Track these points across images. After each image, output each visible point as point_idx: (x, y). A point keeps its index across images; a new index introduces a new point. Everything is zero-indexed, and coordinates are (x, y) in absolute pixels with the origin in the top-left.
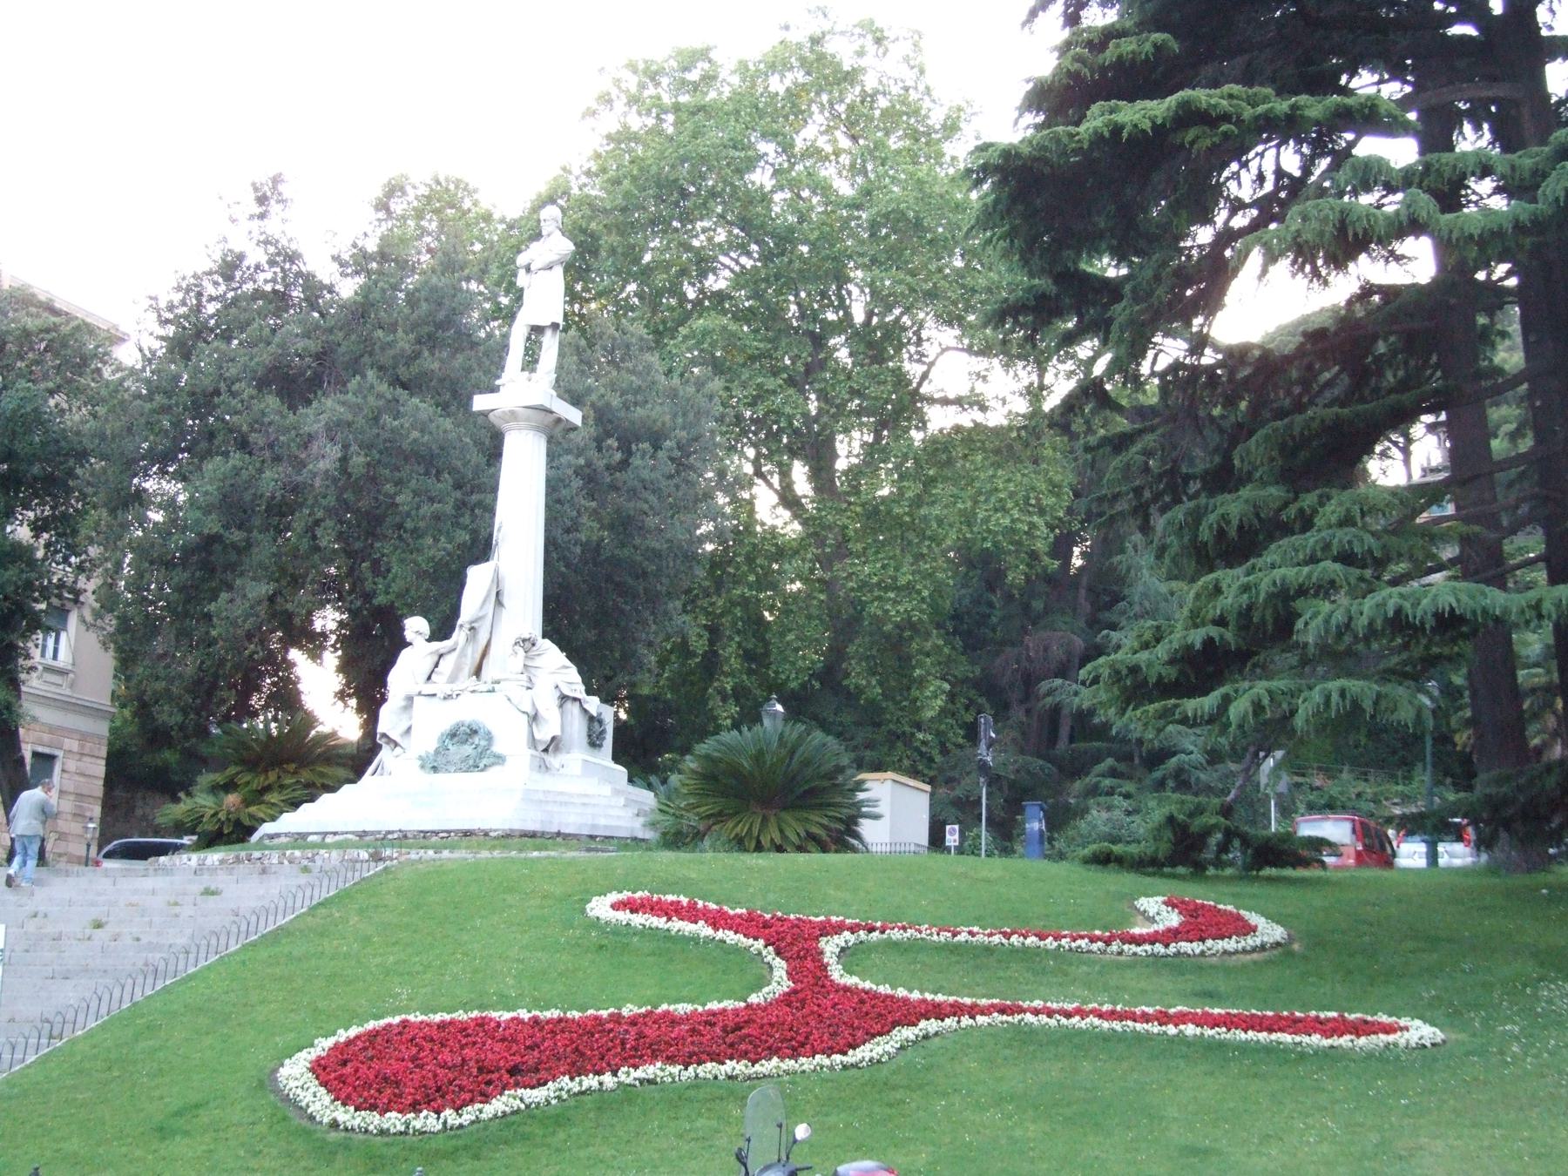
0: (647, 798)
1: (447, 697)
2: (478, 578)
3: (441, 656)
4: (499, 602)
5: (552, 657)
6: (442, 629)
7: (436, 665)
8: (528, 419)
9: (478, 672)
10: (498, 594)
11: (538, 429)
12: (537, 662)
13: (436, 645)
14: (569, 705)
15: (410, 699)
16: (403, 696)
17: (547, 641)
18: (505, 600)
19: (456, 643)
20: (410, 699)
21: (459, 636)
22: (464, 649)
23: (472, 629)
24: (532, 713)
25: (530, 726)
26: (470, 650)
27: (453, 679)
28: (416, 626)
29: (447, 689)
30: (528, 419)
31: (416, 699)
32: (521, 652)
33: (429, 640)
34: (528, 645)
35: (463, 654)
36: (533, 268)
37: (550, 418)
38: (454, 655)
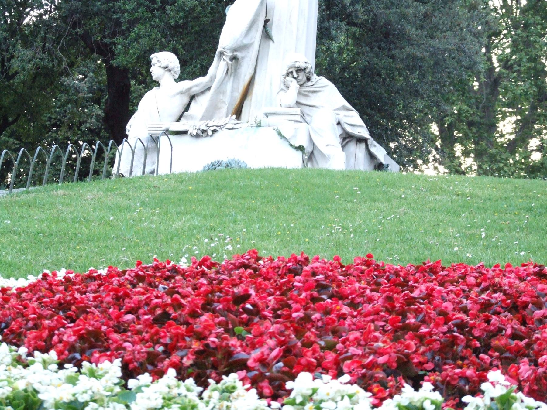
0: (307, 403)
1: (202, 134)
3: (192, 98)
4: (267, 35)
5: (329, 97)
7: (187, 109)
9: (238, 112)
10: (266, 21)
12: (312, 100)
13: (186, 84)
15: (155, 140)
17: (323, 81)
18: (274, 33)
21: (218, 68)
22: (222, 83)
23: (234, 58)
24: (309, 149)
26: (229, 86)
27: (209, 114)
31: (164, 140)
32: (294, 85)
34: (302, 77)
35: (220, 90)
38: (208, 95)
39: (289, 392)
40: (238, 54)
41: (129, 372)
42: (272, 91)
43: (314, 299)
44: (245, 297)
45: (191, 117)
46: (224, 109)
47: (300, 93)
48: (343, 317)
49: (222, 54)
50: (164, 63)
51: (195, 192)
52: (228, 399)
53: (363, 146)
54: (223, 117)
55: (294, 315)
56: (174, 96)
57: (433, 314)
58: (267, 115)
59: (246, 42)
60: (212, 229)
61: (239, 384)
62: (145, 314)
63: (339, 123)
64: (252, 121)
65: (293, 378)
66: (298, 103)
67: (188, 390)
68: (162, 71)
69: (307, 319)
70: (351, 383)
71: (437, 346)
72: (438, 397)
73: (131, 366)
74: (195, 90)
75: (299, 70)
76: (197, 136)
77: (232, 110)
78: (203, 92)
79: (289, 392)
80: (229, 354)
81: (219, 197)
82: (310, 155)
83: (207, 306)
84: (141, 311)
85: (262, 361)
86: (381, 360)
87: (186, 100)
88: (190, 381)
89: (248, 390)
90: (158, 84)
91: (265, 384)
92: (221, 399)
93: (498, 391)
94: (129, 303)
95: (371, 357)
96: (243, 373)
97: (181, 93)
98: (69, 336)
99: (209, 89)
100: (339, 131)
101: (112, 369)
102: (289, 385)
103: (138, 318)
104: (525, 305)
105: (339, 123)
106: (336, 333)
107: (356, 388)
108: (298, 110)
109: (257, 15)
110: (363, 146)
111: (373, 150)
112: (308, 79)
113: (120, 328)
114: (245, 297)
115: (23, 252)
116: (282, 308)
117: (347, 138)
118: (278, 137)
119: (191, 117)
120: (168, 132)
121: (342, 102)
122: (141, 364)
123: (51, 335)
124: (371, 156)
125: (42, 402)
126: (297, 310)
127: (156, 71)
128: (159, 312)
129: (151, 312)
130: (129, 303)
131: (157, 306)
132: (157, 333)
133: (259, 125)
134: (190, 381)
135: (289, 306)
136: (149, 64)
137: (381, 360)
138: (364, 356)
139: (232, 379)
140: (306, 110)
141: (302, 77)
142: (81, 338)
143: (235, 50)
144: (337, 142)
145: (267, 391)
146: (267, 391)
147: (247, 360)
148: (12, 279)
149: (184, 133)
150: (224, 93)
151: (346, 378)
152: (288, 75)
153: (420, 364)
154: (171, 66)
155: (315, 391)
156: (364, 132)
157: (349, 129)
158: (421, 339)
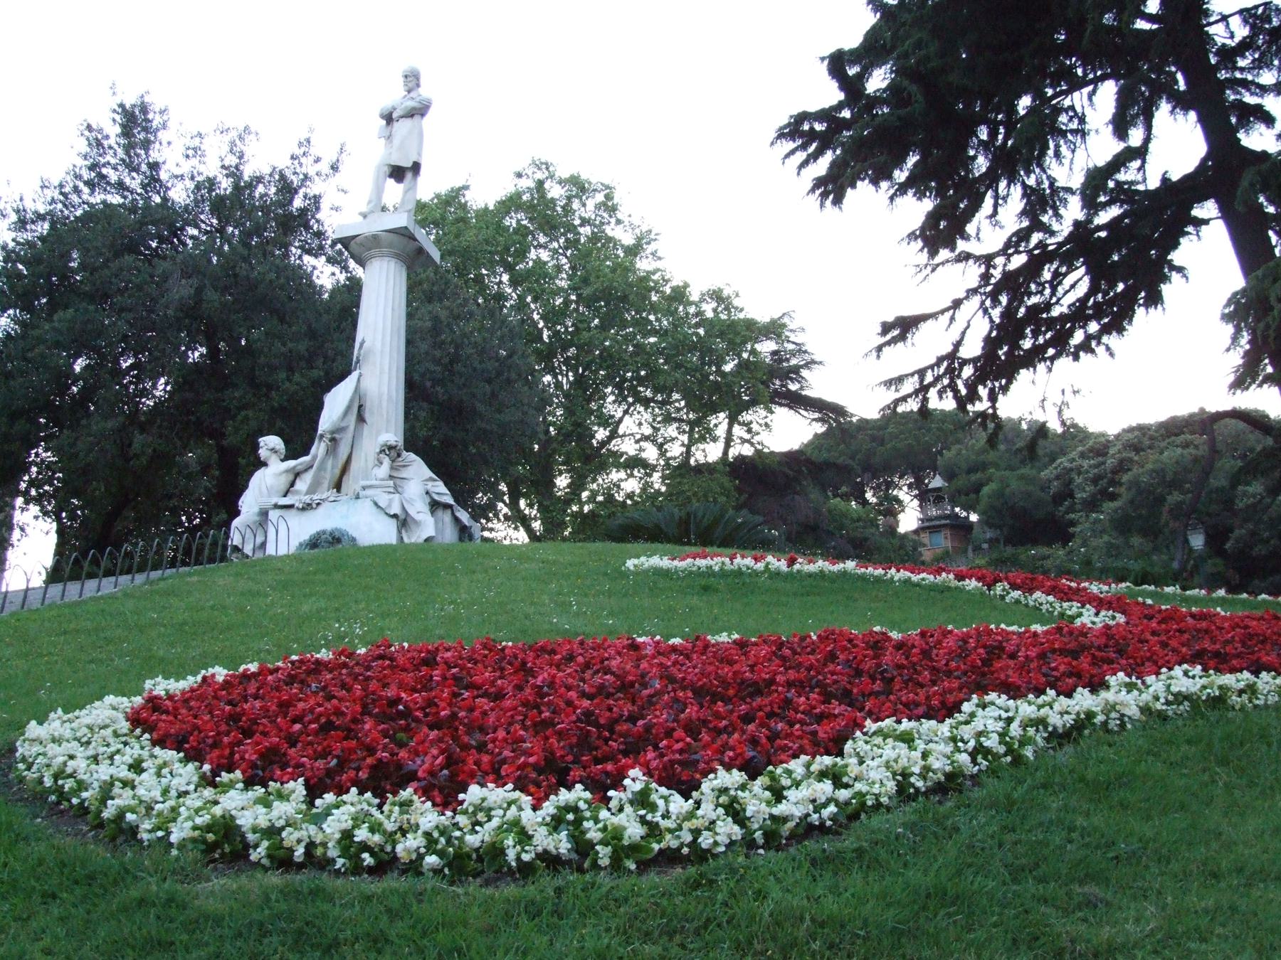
1: (307, 507)
2: (336, 402)
3: (297, 475)
4: (361, 419)
6: (297, 446)
7: (292, 485)
8: (390, 246)
9: (338, 486)
10: (360, 406)
11: (397, 256)
13: (292, 463)
14: (440, 513)
15: (264, 514)
16: (256, 510)
17: (412, 456)
18: (367, 416)
19: (315, 458)
20: (264, 514)
21: (319, 449)
22: (323, 462)
23: (333, 440)
24: (402, 517)
25: (399, 532)
26: (330, 463)
27: (312, 490)
28: (270, 443)
29: (307, 499)
30: (390, 246)
31: (274, 515)
32: (387, 462)
33: (282, 461)
34: (393, 453)
35: (322, 468)
36: (395, 115)
37: (412, 245)
39: (462, 803)
40: (337, 436)
41: (314, 792)
42: (369, 466)
43: (455, 695)
44: (398, 700)
45: (297, 492)
46: (326, 484)
47: (392, 468)
48: (485, 713)
49: (322, 436)
50: (270, 443)
51: (315, 573)
52: (407, 813)
53: (449, 512)
54: (326, 493)
55: (443, 713)
56: (281, 474)
57: (563, 705)
58: (364, 488)
59: (343, 425)
60: (337, 610)
61: (415, 798)
62: (310, 722)
63: (427, 493)
64: (351, 494)
65: (465, 791)
66: (391, 477)
67: (369, 804)
68: (268, 453)
69: (454, 716)
70: (514, 790)
71: (574, 740)
72: (588, 795)
73: (312, 782)
74: (299, 468)
75: (391, 448)
76: (303, 509)
77: (332, 484)
78: (306, 470)
79: (462, 803)
80: (399, 766)
81: (337, 576)
82: (404, 522)
83: (365, 711)
84: (306, 719)
85: (432, 773)
86: (531, 760)
87: (291, 477)
88: (368, 795)
89: (423, 802)
90: (265, 464)
91: (436, 793)
92: (401, 813)
93: (638, 786)
94: (292, 712)
95: (522, 759)
96: (415, 784)
97: (287, 471)
98: (251, 756)
99: (311, 467)
100: (428, 500)
101: (297, 788)
102: (461, 796)
103: (305, 727)
104: (632, 684)
105: (427, 493)
106: (483, 730)
107: (518, 793)
108: (391, 483)
109: (351, 401)
110: (449, 512)
111: (458, 514)
112: (399, 455)
113: (292, 741)
114: (398, 700)
115: (172, 645)
116: (429, 706)
117: (435, 506)
118: (374, 508)
119: (297, 492)
120: (276, 506)
121: (428, 473)
122: (320, 779)
123: (232, 754)
124: (457, 520)
125: (239, 827)
126: (444, 709)
127: (263, 453)
128: (323, 720)
129: (316, 720)
130: (292, 712)
131: (320, 715)
132: (329, 746)
133: (357, 497)
134: (368, 795)
135: (437, 706)
136: (256, 447)
137: (531, 760)
138: (517, 757)
139: (406, 793)
140: (398, 481)
141: (393, 453)
142: (262, 755)
143: (333, 432)
144: (426, 509)
145: (438, 800)
146: (438, 800)
147: (416, 772)
148: (172, 680)
149: (291, 507)
150: (325, 470)
151: (510, 786)
152: (382, 451)
153: (562, 757)
154: (277, 447)
155: (483, 800)
156: (449, 500)
157: (436, 497)
158: (560, 735)
